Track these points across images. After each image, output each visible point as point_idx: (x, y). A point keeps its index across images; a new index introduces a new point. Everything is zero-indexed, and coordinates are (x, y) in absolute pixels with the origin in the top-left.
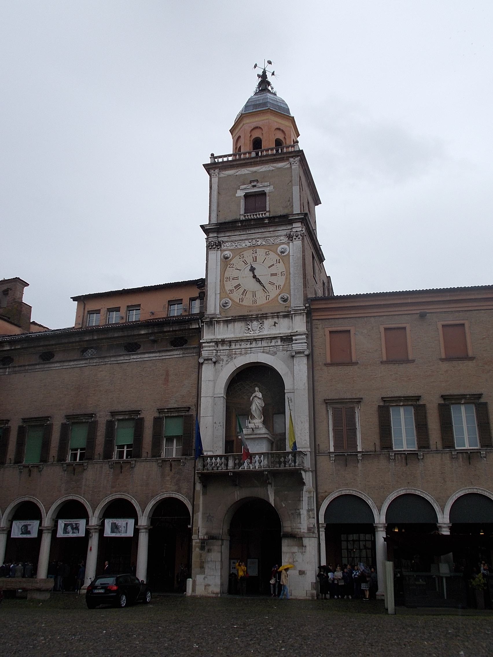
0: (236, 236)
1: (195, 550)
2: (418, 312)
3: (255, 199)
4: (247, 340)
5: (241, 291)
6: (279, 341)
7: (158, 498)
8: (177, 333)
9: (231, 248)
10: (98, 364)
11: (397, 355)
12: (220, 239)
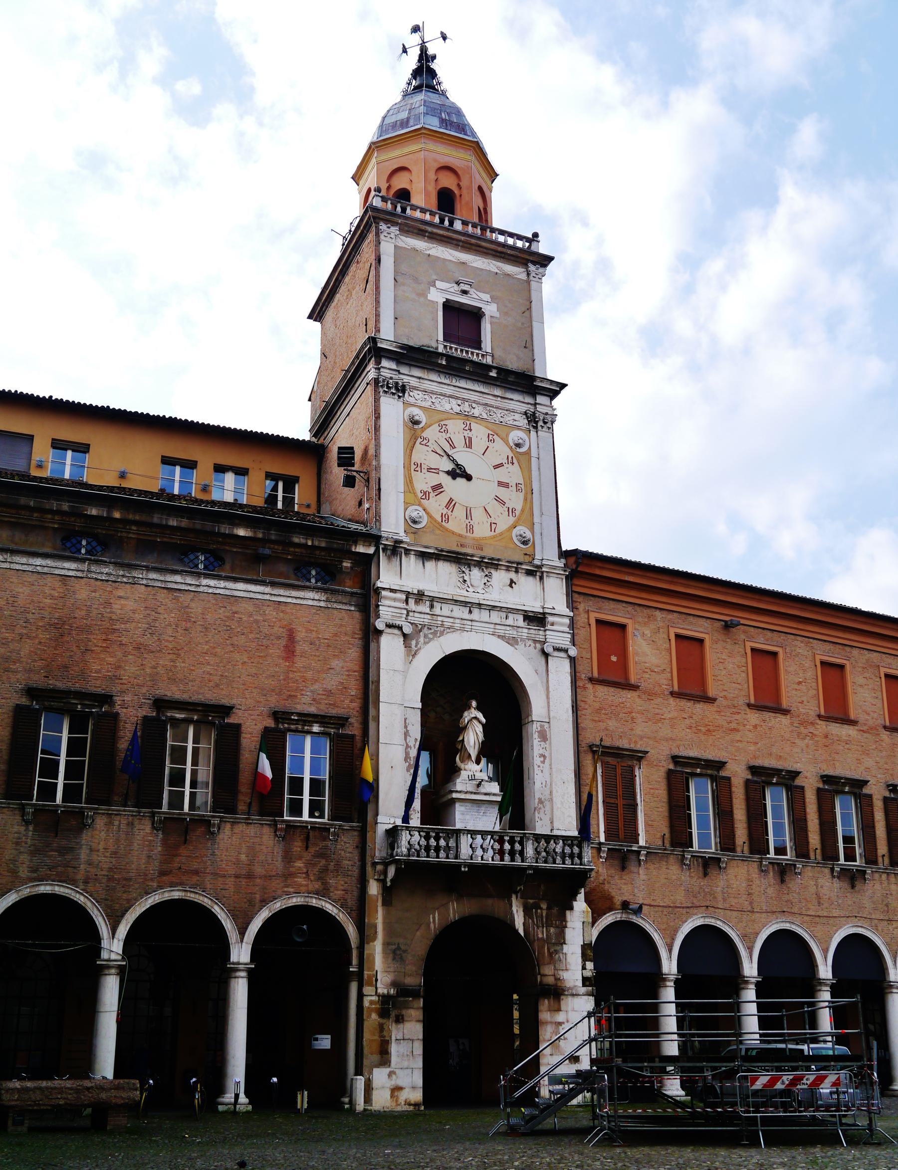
0: (433, 382)
1: (369, 1016)
2: (728, 618)
3: (462, 320)
4: (465, 604)
5: (444, 499)
6: (521, 618)
7: (278, 906)
8: (318, 552)
9: (423, 404)
10: (112, 578)
11: (692, 687)
12: (406, 379)
